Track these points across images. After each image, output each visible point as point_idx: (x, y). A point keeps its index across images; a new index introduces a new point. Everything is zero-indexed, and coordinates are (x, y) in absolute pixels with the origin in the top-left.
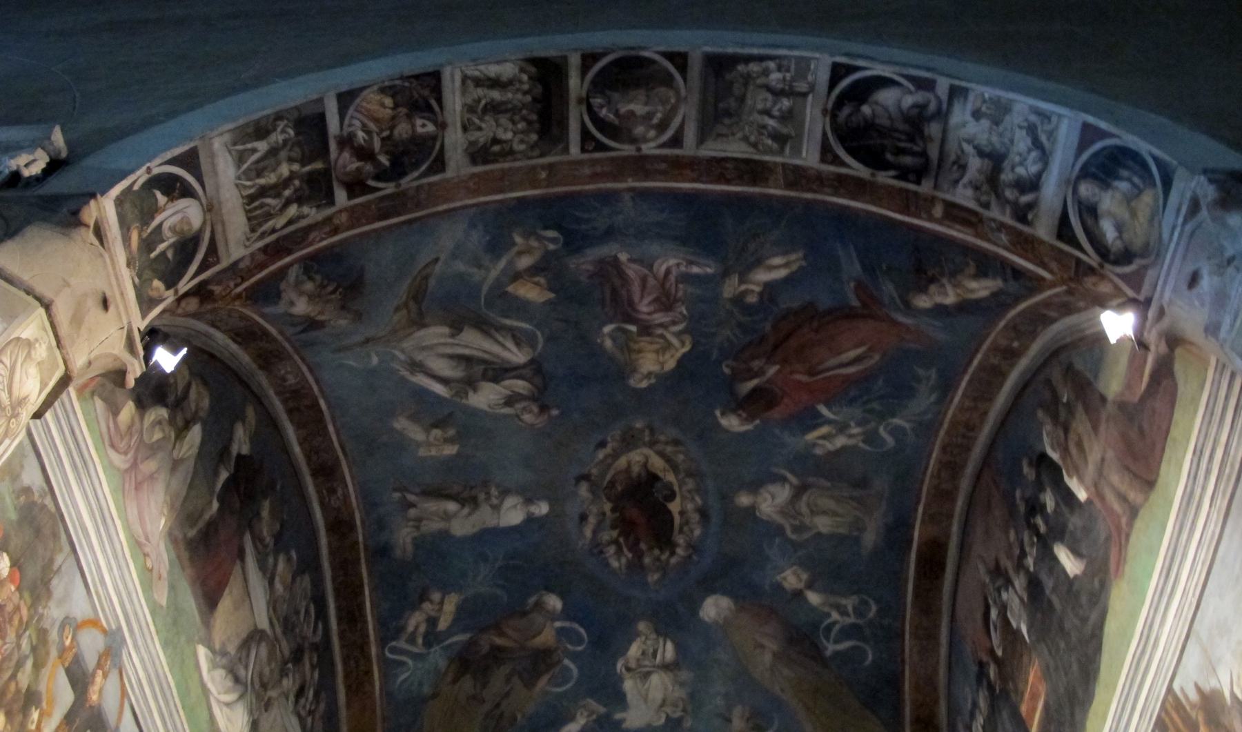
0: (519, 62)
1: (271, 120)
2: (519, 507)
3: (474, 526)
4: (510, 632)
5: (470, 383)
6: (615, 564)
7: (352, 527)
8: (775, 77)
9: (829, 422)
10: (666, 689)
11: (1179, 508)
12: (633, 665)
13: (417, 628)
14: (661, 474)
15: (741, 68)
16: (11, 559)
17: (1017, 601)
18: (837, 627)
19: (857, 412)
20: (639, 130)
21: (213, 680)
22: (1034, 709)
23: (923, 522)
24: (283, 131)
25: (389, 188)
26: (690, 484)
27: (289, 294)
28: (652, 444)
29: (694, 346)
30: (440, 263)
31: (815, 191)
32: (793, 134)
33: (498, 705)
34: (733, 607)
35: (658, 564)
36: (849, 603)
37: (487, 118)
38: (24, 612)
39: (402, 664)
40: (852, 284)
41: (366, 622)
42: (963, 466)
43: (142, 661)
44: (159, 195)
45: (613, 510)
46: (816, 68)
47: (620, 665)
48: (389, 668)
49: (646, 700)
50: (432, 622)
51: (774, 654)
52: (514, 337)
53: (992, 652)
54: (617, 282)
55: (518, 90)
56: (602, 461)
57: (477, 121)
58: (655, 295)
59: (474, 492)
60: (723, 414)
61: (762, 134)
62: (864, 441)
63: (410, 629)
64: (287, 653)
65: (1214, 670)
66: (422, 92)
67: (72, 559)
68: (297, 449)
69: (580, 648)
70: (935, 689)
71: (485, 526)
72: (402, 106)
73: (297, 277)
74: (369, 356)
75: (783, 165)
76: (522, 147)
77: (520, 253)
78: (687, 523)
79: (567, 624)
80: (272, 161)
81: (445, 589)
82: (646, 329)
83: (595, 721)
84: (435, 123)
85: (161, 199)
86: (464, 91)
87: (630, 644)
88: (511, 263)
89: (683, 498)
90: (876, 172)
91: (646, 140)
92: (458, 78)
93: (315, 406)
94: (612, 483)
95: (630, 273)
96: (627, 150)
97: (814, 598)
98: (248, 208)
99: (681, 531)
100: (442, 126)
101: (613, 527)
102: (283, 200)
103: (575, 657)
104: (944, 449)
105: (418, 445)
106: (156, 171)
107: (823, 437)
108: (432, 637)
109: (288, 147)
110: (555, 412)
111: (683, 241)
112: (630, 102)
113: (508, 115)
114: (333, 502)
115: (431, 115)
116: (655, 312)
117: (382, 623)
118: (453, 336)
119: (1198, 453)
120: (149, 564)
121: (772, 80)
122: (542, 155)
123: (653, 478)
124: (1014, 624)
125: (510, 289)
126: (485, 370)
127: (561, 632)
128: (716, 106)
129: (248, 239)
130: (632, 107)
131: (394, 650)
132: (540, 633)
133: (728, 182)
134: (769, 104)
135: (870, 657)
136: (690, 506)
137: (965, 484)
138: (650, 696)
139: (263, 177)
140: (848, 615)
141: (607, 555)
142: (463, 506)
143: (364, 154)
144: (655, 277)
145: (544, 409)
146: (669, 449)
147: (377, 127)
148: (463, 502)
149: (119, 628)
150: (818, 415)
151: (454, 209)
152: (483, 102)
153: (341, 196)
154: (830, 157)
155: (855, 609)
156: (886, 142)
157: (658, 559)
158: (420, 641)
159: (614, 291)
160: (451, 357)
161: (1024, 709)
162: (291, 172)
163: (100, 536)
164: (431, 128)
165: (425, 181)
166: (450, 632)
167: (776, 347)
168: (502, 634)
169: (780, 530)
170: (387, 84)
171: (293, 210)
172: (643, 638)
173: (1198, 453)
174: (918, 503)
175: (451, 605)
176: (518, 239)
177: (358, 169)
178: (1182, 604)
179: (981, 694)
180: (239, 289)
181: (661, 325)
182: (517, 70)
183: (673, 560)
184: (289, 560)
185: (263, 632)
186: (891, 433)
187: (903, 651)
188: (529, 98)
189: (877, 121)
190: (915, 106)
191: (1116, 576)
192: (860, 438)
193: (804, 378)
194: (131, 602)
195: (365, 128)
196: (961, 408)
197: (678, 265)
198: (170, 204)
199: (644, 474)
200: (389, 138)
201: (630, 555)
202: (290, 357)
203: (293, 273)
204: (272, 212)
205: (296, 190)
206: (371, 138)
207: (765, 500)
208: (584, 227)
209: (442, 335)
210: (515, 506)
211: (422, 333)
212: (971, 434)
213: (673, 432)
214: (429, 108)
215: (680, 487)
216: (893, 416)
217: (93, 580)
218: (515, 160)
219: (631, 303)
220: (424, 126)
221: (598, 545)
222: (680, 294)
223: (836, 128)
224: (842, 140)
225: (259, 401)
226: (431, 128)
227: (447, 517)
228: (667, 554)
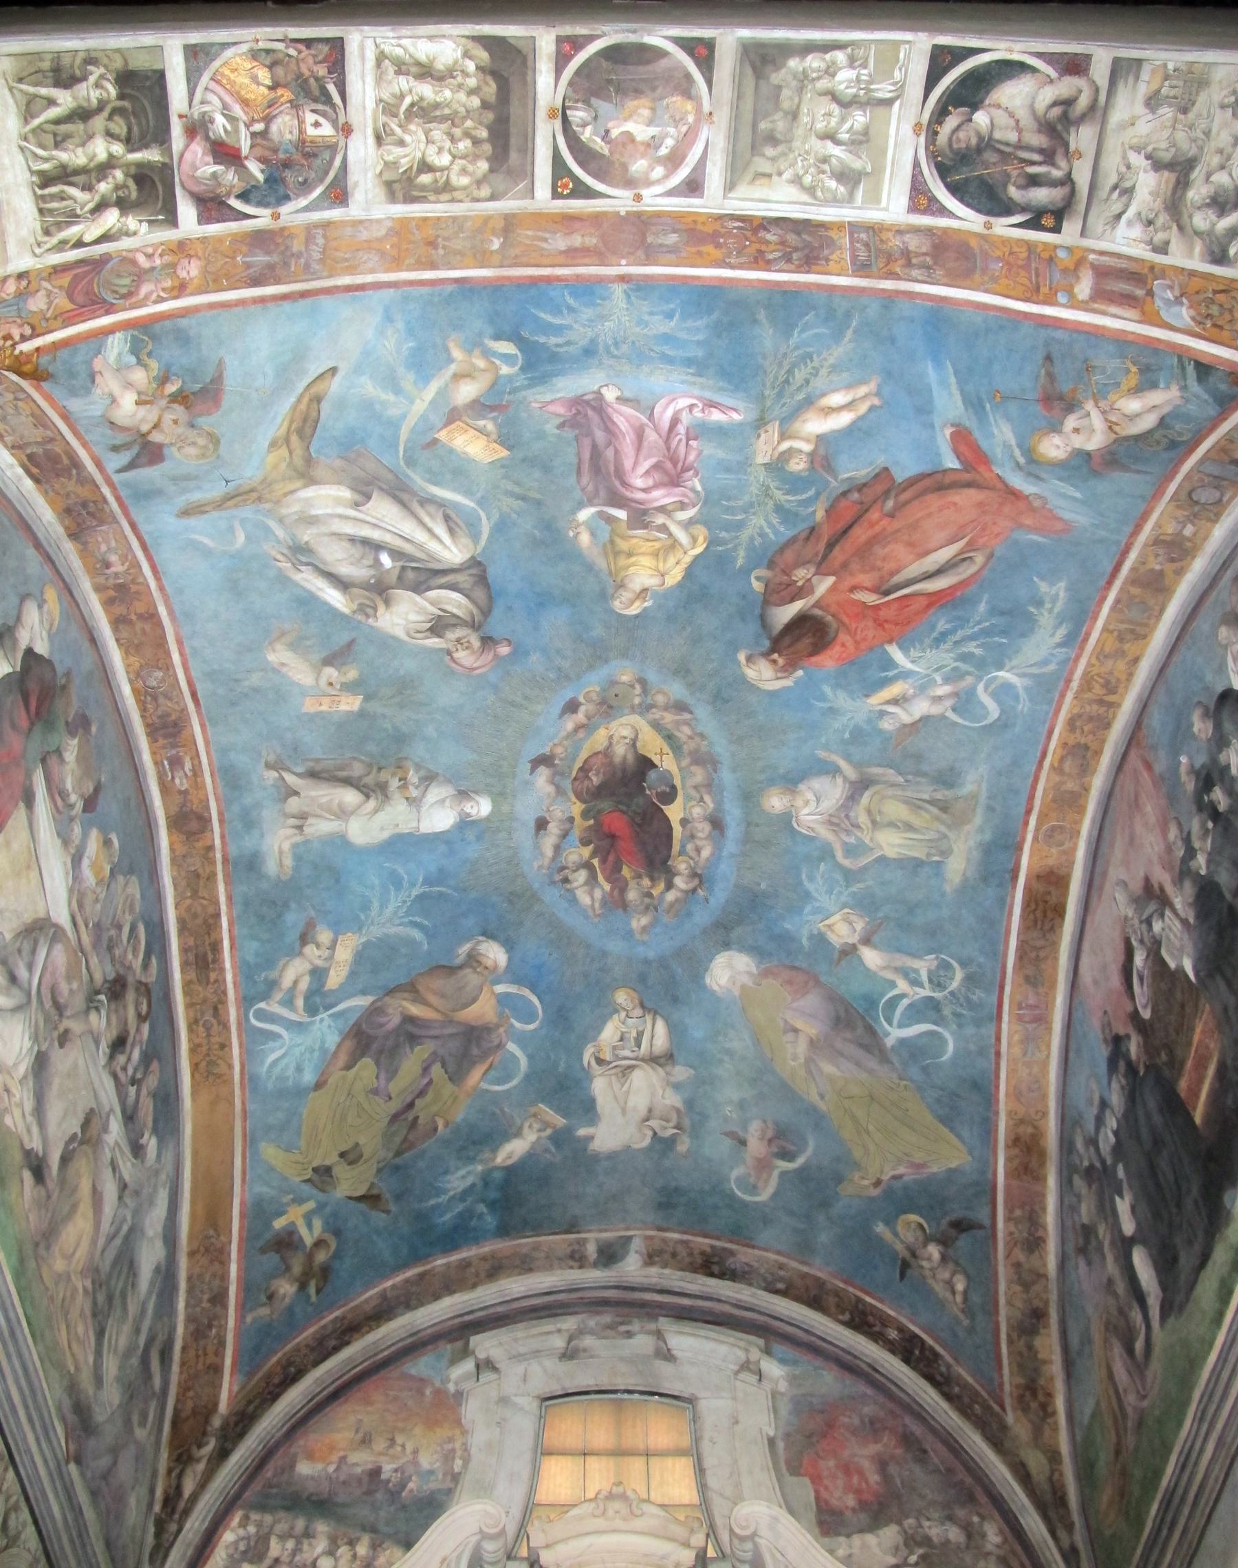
0: (464, 40)
1: (78, 61)
2: (447, 803)
3: (382, 829)
4: (433, 999)
5: (380, 590)
6: (585, 899)
7: (205, 821)
8: (845, 75)
9: (905, 675)
10: (653, 1094)
12: (608, 1056)
13: (296, 982)
14: (656, 760)
15: (793, 63)
17: (1177, 926)
19: (945, 657)
20: (638, 166)
22: (1200, 1081)
23: (1035, 839)
24: (97, 85)
25: (262, 218)
26: (699, 775)
27: (109, 383)
28: (644, 709)
29: (712, 542)
30: (338, 378)
31: (897, 277)
32: (869, 169)
33: (411, 1105)
34: (754, 970)
35: (647, 900)
36: (923, 966)
37: (412, 127)
39: (275, 1036)
40: (948, 432)
41: (222, 970)
42: (1098, 753)
45: (585, 815)
46: (908, 57)
47: (588, 1055)
48: (255, 1039)
49: (624, 1111)
50: (318, 974)
51: (812, 1043)
52: (447, 518)
53: (1135, 1016)
54: (600, 435)
55: (460, 86)
56: (567, 737)
57: (398, 130)
58: (653, 461)
59: (384, 776)
60: (749, 659)
61: (824, 172)
62: (954, 710)
63: (287, 982)
64: (98, 977)
66: (315, 69)
68: (127, 690)
69: (532, 1027)
70: (1044, 1097)
71: (397, 831)
72: (285, 86)
73: (120, 354)
74: (231, 530)
75: (854, 227)
76: (465, 181)
77: (457, 377)
78: (692, 837)
79: (512, 989)
80: (78, 128)
81: (338, 928)
82: (640, 517)
83: (550, 1138)
84: (334, 123)
86: (379, 80)
87: (604, 1023)
88: (442, 393)
89: (688, 798)
90: (992, 219)
91: (649, 183)
92: (371, 55)
93: (152, 617)
94: (584, 769)
95: (618, 419)
96: (618, 200)
97: (871, 958)
98: (39, 192)
99: (682, 852)
100: (347, 130)
101: (585, 842)
102: (97, 198)
103: (522, 1040)
104: (1071, 724)
105: (304, 692)
107: (895, 702)
108: (317, 999)
109: (105, 114)
110: (504, 650)
111: (698, 366)
112: (626, 120)
113: (445, 126)
114: (177, 781)
115: (327, 109)
116: (656, 486)
117: (247, 972)
118: (357, 505)
121: (840, 83)
122: (493, 197)
123: (645, 764)
124: (1172, 965)
125: (442, 435)
126: (403, 568)
127: (503, 999)
128: (754, 126)
129: (39, 245)
130: (630, 126)
131: (262, 1016)
132: (474, 1000)
133: (767, 265)
134: (834, 122)
135: (951, 1047)
136: (697, 811)
137: (1098, 783)
138: (630, 1104)
139: (65, 150)
140: (922, 986)
141: (575, 884)
142: (368, 797)
143: (224, 153)
144: (656, 429)
145: (488, 641)
146: (669, 718)
147: (246, 113)
148: (367, 793)
150: (889, 663)
151: (362, 287)
152: (408, 101)
153: (187, 211)
154: (924, 201)
155: (930, 972)
156: (1009, 168)
157: (649, 895)
158: (300, 1002)
159: (596, 453)
160: (352, 540)
161: (1183, 1085)
162: (111, 156)
164: (327, 130)
165: (316, 216)
166: (345, 991)
167: (830, 546)
168: (419, 999)
169: (826, 853)
170: (261, 45)
171: (111, 218)
172: (623, 1014)
174: (1029, 812)
175: (344, 954)
176: (457, 354)
177: (214, 176)
179: (1115, 1085)
181: (662, 509)
182: (459, 54)
183: (671, 896)
184: (107, 843)
185: (56, 926)
186: (995, 695)
187: (998, 1039)
188: (475, 102)
189: (997, 135)
190: (1055, 104)
192: (949, 703)
193: (870, 599)
195: (225, 108)
196: (1101, 654)
197: (691, 407)
199: (630, 758)
200: (264, 134)
201: (607, 887)
202: (115, 520)
203: (116, 345)
204: (79, 212)
205: (117, 188)
206: (236, 130)
207: (807, 803)
208: (553, 340)
209: (338, 501)
210: (442, 801)
211: (309, 492)
212: (1111, 698)
213: (677, 690)
214: (328, 100)
215: (683, 779)
216: (1000, 667)
218: (453, 200)
219: (620, 473)
220: (317, 124)
221: (563, 868)
222: (692, 457)
223: (932, 155)
224: (943, 171)
225: (68, 590)
226: (327, 130)
227: (343, 813)
228: (662, 886)
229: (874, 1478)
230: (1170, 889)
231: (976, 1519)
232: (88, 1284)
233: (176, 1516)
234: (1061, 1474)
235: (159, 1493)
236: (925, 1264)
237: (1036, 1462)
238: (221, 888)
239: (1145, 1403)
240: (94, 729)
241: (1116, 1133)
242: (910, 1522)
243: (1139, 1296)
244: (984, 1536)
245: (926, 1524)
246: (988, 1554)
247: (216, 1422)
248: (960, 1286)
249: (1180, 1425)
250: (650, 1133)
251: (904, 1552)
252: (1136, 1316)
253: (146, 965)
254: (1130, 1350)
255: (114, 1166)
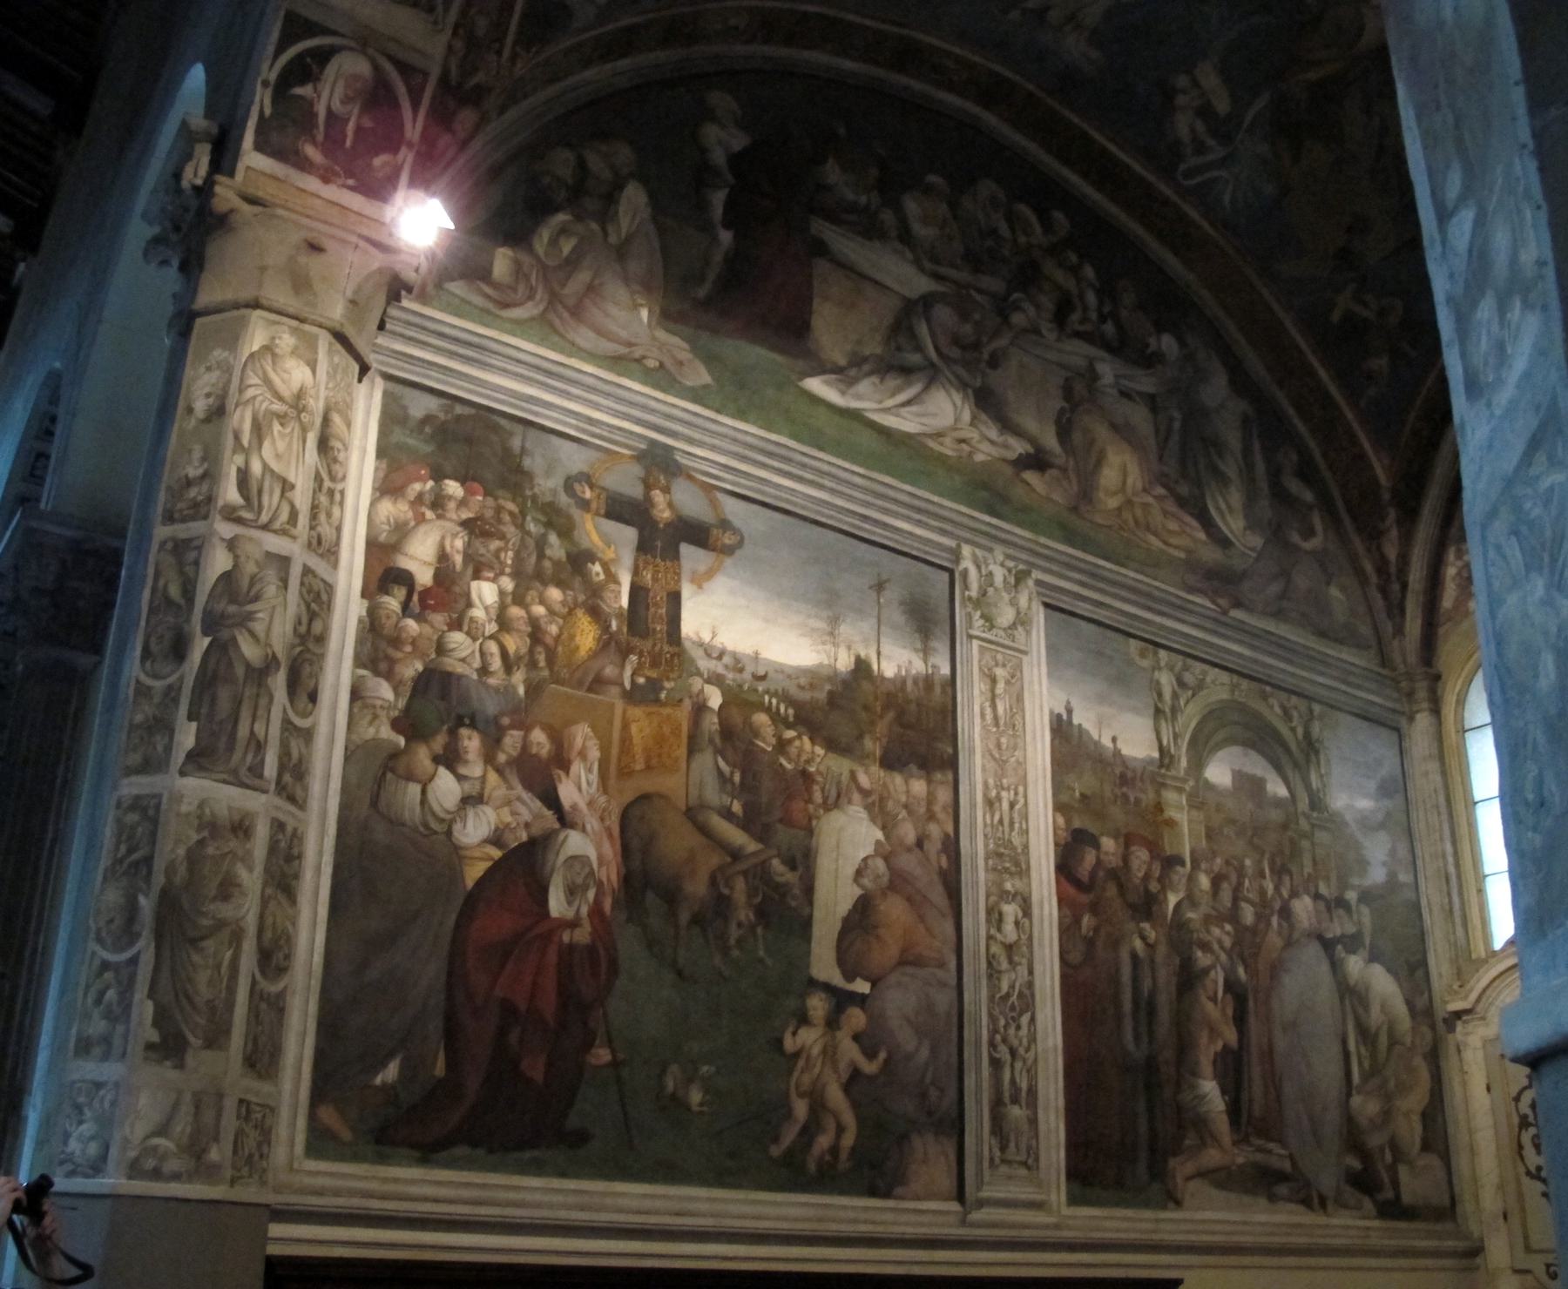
13: (1193, 130)
16: (456, 479)
21: (859, 397)
38: (511, 506)
43: (713, 448)
44: (298, 91)
50: (1205, 111)
67: (533, 434)
68: (848, 65)
85: (305, 91)
106: (273, 76)
120: (651, 363)
149: (653, 443)
158: (1211, 142)
163: (555, 388)
180: (506, 53)
194: (653, 411)
198: (319, 86)
217: (577, 429)
232: (1160, 491)
233: (1394, 578)
235: (1369, 567)
238: (1067, 113)
240: (842, 131)
247: (1386, 496)
253: (1048, 226)
255: (1125, 394)
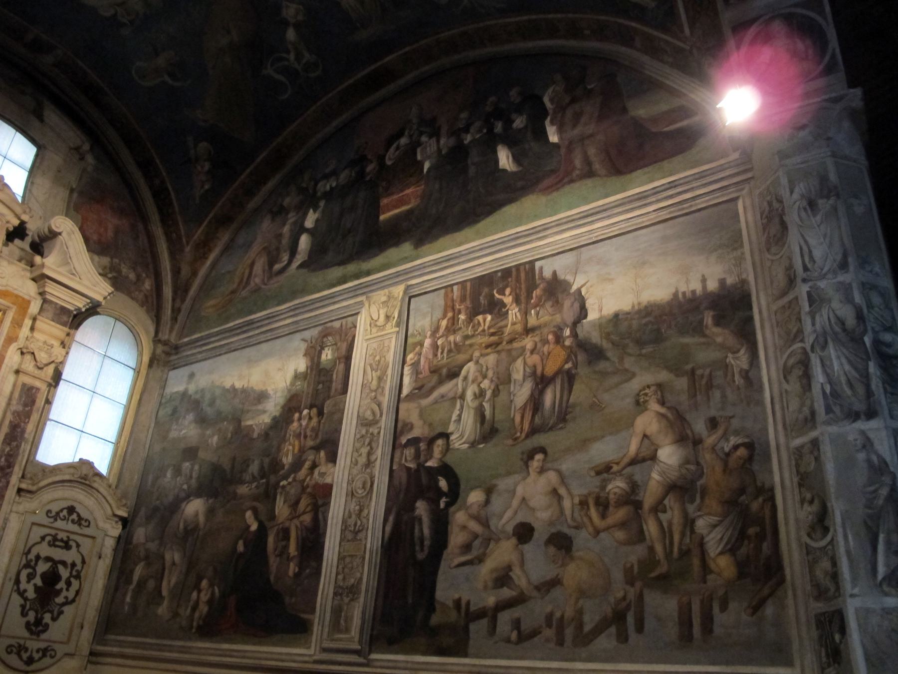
11: (629, 197)
18: (286, 63)
22: (396, 207)
65: (576, 273)
97: (291, 34)
119: (672, 185)
124: (419, 158)
161: (384, 201)
173: (672, 185)
178: (584, 234)
191: (540, 191)
229: (110, 234)
230: (444, 131)
231: (144, 275)
234: (193, 281)
236: (199, 168)
237: (185, 270)
239: (263, 286)
241: (332, 188)
242: (116, 261)
243: (293, 251)
244: (143, 283)
245: (123, 265)
246: (141, 291)
248: (207, 187)
249: (279, 304)
250: (112, 12)
251: (108, 271)
252: (285, 258)
254: (271, 264)
